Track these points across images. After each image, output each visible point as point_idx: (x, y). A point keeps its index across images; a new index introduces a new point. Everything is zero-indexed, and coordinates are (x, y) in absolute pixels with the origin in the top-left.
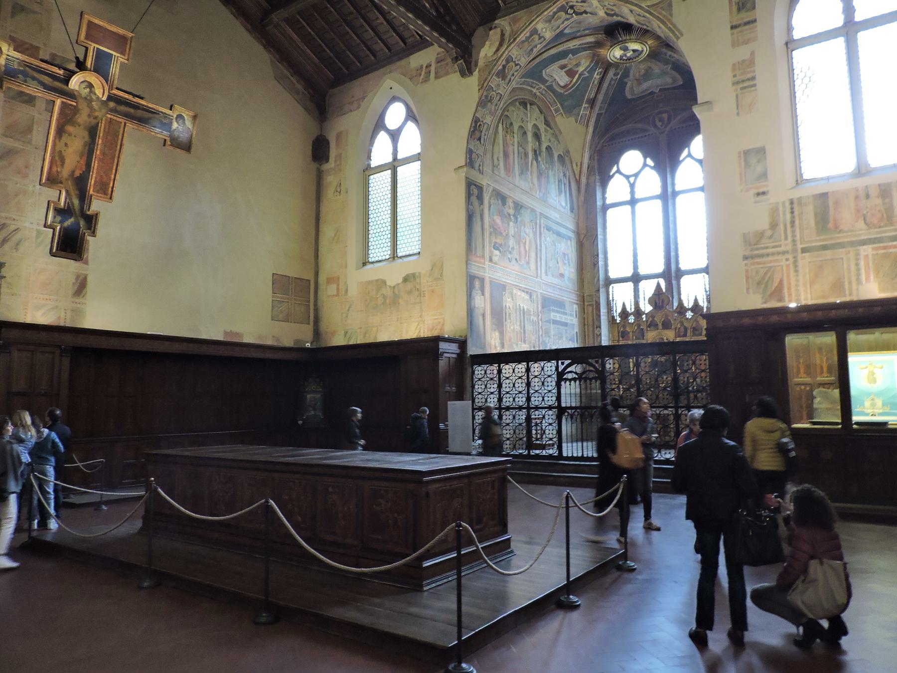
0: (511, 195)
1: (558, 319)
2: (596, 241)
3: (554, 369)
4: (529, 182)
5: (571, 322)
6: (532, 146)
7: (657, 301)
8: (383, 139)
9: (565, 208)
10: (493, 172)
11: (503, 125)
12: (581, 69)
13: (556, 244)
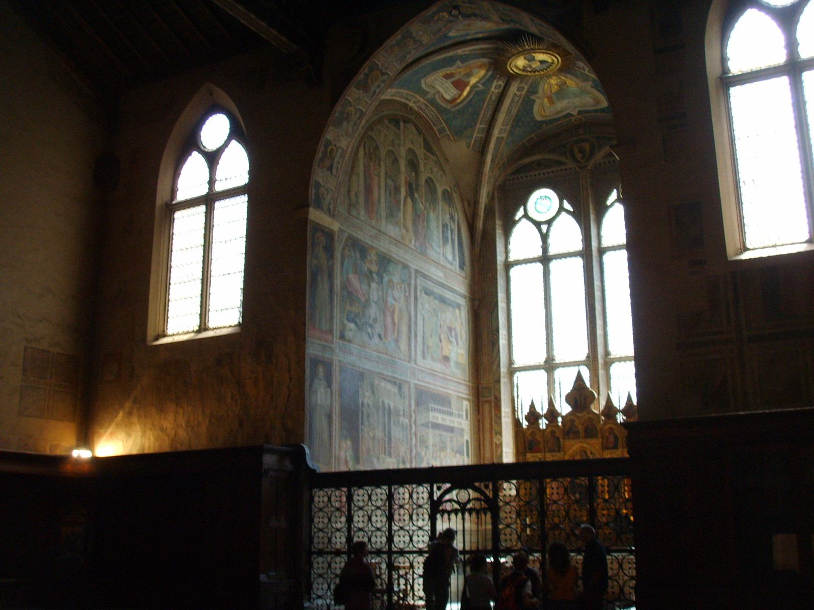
0: (375, 245)
1: (440, 421)
3: (426, 495)
4: (400, 227)
5: (460, 427)
9: (451, 264)
10: (349, 213)
11: (364, 149)
12: (473, 81)
13: (439, 315)
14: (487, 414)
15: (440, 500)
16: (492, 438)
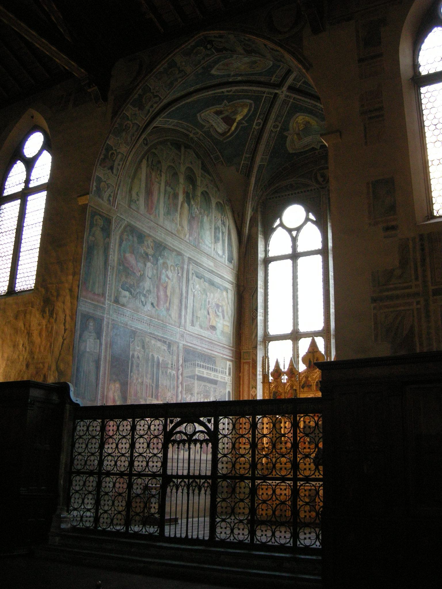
0: (151, 234)
1: (205, 375)
2: (255, 293)
4: (176, 224)
5: (223, 381)
6: (184, 189)
7: (312, 360)
8: (19, 168)
9: (222, 257)
10: (130, 207)
11: (148, 161)
12: (239, 118)
13: (208, 294)
14: (246, 373)
15: (172, 433)
16: (249, 391)
